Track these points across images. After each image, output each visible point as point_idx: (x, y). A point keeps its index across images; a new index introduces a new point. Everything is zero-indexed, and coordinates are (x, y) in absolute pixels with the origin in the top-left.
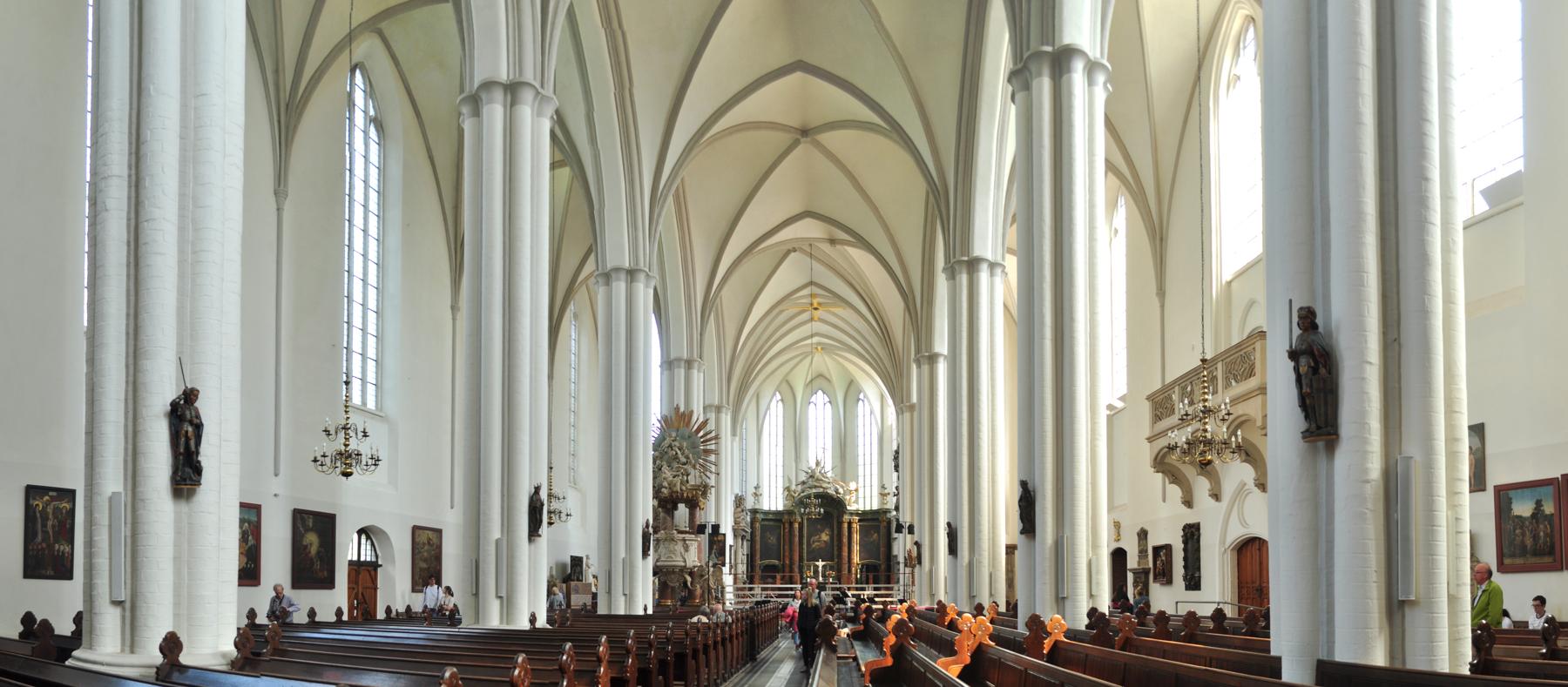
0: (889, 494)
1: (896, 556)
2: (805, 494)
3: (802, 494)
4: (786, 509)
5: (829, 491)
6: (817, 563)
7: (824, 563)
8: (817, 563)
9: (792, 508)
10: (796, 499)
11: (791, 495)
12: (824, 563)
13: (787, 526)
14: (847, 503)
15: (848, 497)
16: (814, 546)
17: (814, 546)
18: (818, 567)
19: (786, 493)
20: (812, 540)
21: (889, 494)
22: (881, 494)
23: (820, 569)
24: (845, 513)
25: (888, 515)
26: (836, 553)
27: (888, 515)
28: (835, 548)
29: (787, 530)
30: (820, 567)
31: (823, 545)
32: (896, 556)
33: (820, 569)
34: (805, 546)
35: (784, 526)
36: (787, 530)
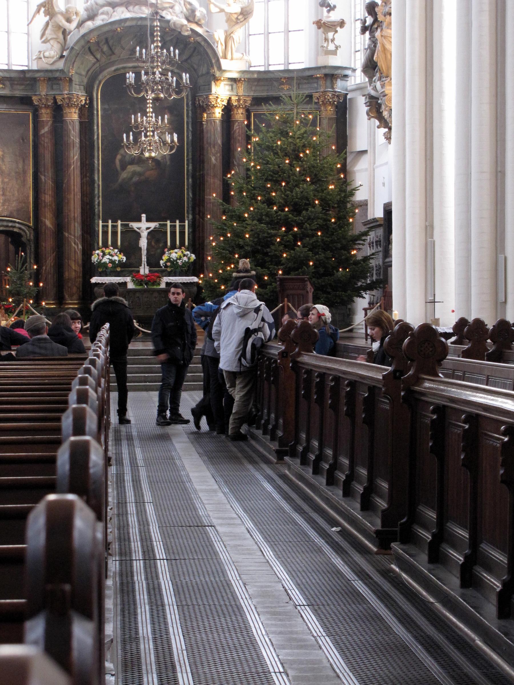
0: (342, 24)
1: (364, 205)
2: (99, 22)
3: (90, 25)
4: (44, 65)
5: (167, 15)
6: (135, 225)
7: (153, 225)
8: (135, 225)
9: (60, 65)
10: (72, 40)
11: (58, 27)
12: (153, 225)
13: (46, 115)
14: (220, 50)
15: (219, 35)
16: (124, 175)
17: (124, 175)
18: (138, 236)
19: (42, 19)
20: (119, 157)
21: (342, 24)
22: (319, 24)
23: (143, 243)
24: (216, 80)
25: (340, 86)
26: (188, 194)
27: (340, 86)
28: (187, 182)
29: (45, 130)
30: (144, 234)
31: (152, 174)
32: (364, 205)
33: (143, 243)
34: (98, 178)
35: (36, 117)
36: (45, 130)
